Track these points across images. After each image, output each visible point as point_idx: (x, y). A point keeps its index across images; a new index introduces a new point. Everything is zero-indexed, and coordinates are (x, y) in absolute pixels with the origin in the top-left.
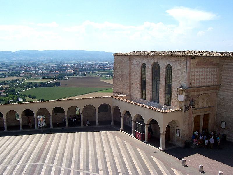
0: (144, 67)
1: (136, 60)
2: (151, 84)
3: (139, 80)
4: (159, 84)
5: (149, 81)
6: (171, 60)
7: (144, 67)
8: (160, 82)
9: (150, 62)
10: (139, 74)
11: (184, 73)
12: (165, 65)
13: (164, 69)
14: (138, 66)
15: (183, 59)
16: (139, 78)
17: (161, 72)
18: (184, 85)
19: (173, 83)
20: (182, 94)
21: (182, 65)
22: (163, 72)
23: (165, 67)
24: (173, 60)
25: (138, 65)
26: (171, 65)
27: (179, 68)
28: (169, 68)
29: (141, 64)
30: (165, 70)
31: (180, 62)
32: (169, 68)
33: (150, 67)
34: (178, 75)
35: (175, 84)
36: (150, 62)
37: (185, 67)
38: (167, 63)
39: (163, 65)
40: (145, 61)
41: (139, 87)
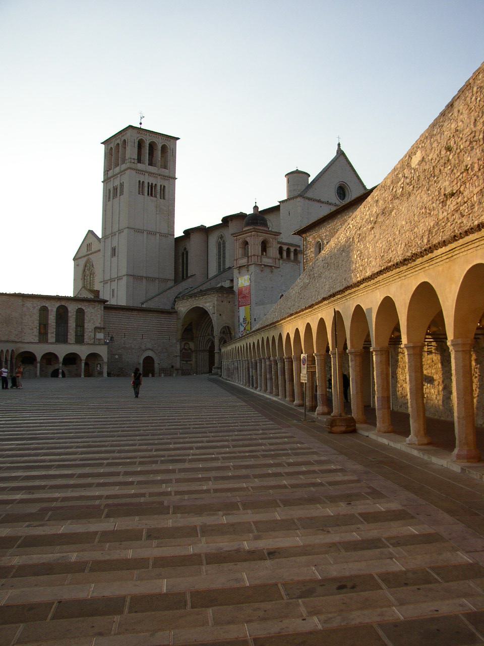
0: (44, 311)
3: (37, 323)
4: (68, 326)
5: (53, 324)
6: (83, 304)
7: (44, 311)
8: (69, 325)
9: (54, 305)
10: (36, 317)
12: (75, 308)
13: (74, 312)
14: (34, 309)
16: (38, 322)
17: (69, 315)
18: (98, 325)
19: (86, 325)
20: (100, 332)
21: (96, 309)
22: (73, 315)
23: (75, 310)
24: (86, 304)
25: (34, 308)
26: (84, 308)
27: (93, 311)
28: (80, 313)
31: (93, 306)
32: (80, 313)
33: (55, 310)
34: (92, 318)
35: (88, 326)
36: (54, 305)
38: (78, 307)
39: (72, 308)
40: (47, 304)
41: (36, 332)
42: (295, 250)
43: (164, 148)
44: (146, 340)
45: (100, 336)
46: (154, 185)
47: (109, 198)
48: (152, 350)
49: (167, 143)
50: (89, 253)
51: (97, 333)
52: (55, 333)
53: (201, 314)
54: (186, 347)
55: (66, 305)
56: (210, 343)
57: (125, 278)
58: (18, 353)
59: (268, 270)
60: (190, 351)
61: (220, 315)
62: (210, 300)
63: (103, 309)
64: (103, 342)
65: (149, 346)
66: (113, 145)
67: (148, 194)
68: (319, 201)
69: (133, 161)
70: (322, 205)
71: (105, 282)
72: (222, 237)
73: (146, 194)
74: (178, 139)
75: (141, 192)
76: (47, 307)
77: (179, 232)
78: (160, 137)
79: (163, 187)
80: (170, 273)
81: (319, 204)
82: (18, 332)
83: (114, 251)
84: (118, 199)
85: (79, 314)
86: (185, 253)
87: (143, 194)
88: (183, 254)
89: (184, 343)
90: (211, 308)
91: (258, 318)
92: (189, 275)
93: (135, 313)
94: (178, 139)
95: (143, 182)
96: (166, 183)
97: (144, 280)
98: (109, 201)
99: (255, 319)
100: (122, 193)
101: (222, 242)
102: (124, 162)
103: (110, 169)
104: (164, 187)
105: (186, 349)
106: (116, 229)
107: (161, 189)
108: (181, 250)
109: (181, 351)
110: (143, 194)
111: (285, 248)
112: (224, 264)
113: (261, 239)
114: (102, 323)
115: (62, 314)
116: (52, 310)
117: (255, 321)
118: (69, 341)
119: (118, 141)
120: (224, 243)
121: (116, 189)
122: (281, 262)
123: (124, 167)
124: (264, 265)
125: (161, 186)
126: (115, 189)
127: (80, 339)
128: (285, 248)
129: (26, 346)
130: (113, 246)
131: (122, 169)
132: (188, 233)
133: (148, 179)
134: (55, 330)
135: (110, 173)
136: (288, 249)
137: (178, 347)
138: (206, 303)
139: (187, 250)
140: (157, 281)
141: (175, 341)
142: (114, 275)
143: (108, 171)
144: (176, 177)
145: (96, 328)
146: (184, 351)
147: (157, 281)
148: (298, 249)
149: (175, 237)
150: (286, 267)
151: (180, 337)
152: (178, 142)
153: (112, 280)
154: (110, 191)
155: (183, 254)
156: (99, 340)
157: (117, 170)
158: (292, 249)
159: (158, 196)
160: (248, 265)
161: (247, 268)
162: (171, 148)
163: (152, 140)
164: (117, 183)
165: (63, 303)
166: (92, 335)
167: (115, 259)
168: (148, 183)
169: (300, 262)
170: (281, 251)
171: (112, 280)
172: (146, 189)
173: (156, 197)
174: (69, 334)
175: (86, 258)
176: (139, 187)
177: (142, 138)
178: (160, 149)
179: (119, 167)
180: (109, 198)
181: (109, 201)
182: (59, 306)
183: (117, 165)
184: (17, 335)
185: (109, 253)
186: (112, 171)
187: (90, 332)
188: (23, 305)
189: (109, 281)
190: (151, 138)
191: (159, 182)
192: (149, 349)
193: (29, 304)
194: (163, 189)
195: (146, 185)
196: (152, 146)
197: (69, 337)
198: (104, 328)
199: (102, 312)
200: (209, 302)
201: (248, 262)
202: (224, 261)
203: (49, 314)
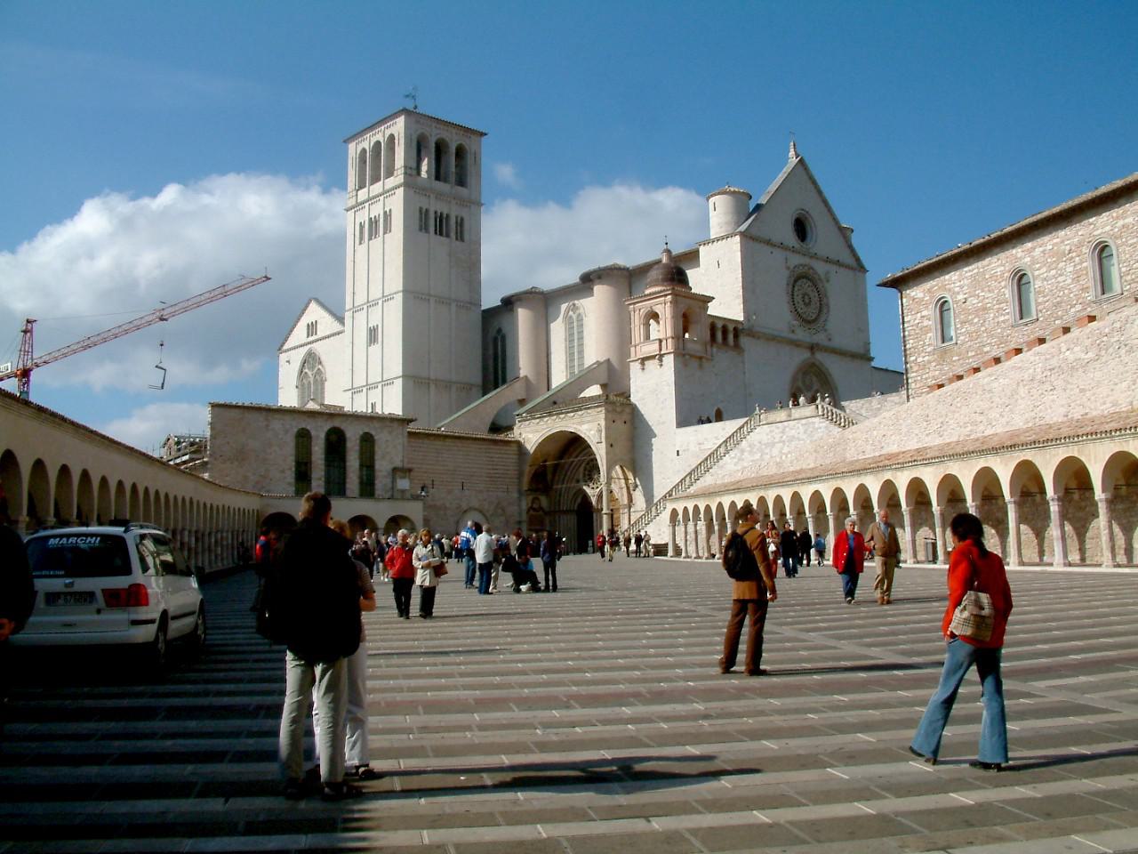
0: (304, 437)
1: (281, 421)
2: (323, 467)
3: (290, 462)
4: (344, 468)
7: (304, 437)
8: (348, 464)
11: (400, 448)
15: (395, 425)
16: (293, 458)
17: (349, 445)
18: (398, 464)
19: (377, 466)
20: (404, 478)
23: (358, 437)
24: (376, 424)
25: (287, 432)
26: (373, 433)
28: (368, 441)
29: (296, 430)
30: (358, 441)
33: (323, 435)
37: (400, 436)
39: (353, 435)
40: (308, 424)
41: (290, 476)
42: (735, 329)
43: (460, 153)
44: (467, 492)
45: (403, 484)
46: (445, 216)
47: (361, 238)
48: (481, 512)
49: (466, 142)
50: (311, 339)
51: (398, 480)
52: (323, 479)
53: (573, 444)
54: (535, 506)
55: (342, 427)
56: (579, 500)
57: (399, 383)
58: (267, 515)
59: (695, 363)
60: (541, 513)
61: (611, 445)
62: (589, 419)
63: (406, 434)
64: (408, 495)
65: (475, 504)
66: (367, 143)
67: (436, 233)
68: (768, 243)
69: (409, 171)
70: (774, 250)
71: (355, 391)
72: (575, 308)
73: (432, 229)
74: (486, 134)
75: (424, 227)
76: (308, 431)
77: (490, 300)
78: (454, 131)
79: (459, 219)
80: (476, 377)
81: (768, 249)
82: (261, 476)
83: (373, 336)
84: (380, 239)
85: (364, 443)
86: (499, 337)
87: (427, 230)
88: (495, 339)
89: (531, 497)
90: (592, 432)
91: (684, 451)
92: (509, 377)
93: (449, 442)
94: (483, 134)
95: (427, 210)
96: (464, 213)
97: (433, 387)
98: (360, 243)
99: (678, 451)
100: (387, 229)
101: (574, 317)
102: (390, 173)
103: (361, 188)
104: (462, 219)
105: (534, 509)
106: (376, 293)
107: (457, 222)
108: (492, 333)
109: (528, 511)
110: (427, 230)
111: (719, 325)
112: (581, 357)
113: (682, 308)
114: (406, 460)
115: (336, 443)
116: (318, 436)
117: (678, 455)
118: (348, 493)
119: (379, 137)
120: (580, 319)
121: (376, 222)
122: (715, 350)
123: (390, 182)
124: (689, 355)
125: (457, 217)
126: (373, 223)
127: (368, 489)
128: (719, 325)
129: (276, 502)
130: (371, 325)
131: (387, 187)
132: (509, 303)
133: (436, 206)
134: (323, 473)
135: (363, 195)
136: (725, 331)
137: (525, 504)
138: (582, 423)
139: (504, 331)
140: (454, 389)
141: (515, 495)
142: (375, 377)
143: (358, 190)
144: (483, 202)
145: (395, 470)
146: (532, 512)
147: (454, 389)
148: (740, 327)
149: (483, 308)
150: (723, 358)
151: (525, 487)
152: (484, 139)
153: (370, 387)
154: (362, 227)
155: (495, 339)
156: (403, 491)
157: (377, 188)
158: (731, 327)
159: (453, 235)
160: (661, 356)
161: (661, 360)
162: (473, 151)
163: (439, 136)
164: (377, 210)
165: (337, 423)
166: (389, 481)
167: (375, 349)
168: (436, 212)
169: (743, 351)
170: (713, 328)
171: (370, 387)
172: (432, 222)
173: (448, 236)
174: (348, 480)
175: (306, 349)
176: (421, 220)
177: (423, 131)
178: (454, 151)
179: (381, 182)
180: (361, 238)
181: (360, 243)
182: (329, 430)
183: (375, 179)
184: (257, 483)
185: (362, 335)
186: (366, 190)
187: (385, 477)
188: (267, 426)
189: (365, 389)
190: (438, 132)
191: (454, 211)
192: (476, 509)
193: (276, 424)
194: (460, 223)
195: (432, 216)
196: (440, 149)
197: (348, 486)
198: (410, 470)
199: (406, 440)
200: (589, 422)
201: (661, 350)
202: (581, 352)
203: (313, 444)
